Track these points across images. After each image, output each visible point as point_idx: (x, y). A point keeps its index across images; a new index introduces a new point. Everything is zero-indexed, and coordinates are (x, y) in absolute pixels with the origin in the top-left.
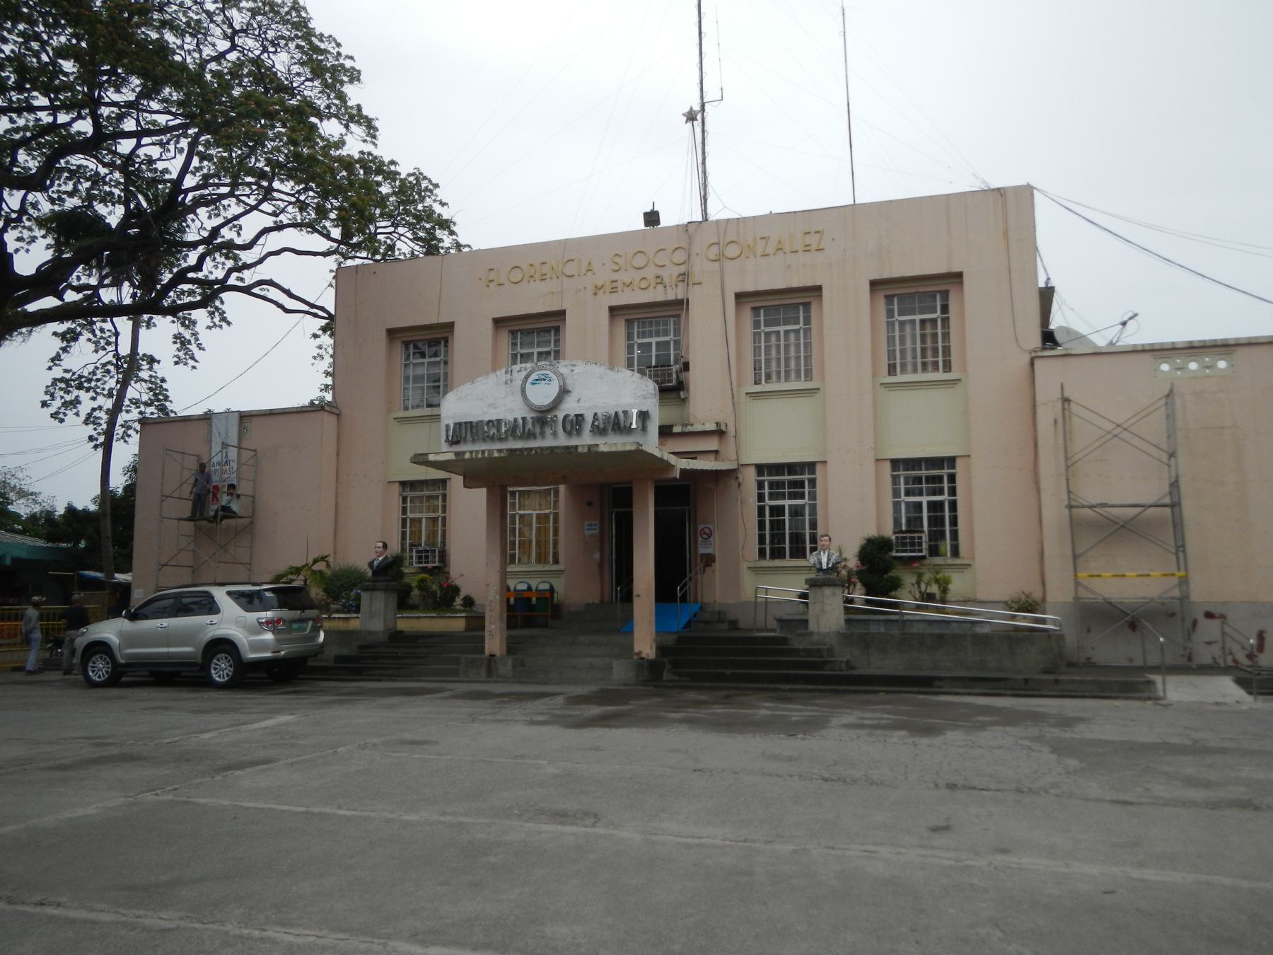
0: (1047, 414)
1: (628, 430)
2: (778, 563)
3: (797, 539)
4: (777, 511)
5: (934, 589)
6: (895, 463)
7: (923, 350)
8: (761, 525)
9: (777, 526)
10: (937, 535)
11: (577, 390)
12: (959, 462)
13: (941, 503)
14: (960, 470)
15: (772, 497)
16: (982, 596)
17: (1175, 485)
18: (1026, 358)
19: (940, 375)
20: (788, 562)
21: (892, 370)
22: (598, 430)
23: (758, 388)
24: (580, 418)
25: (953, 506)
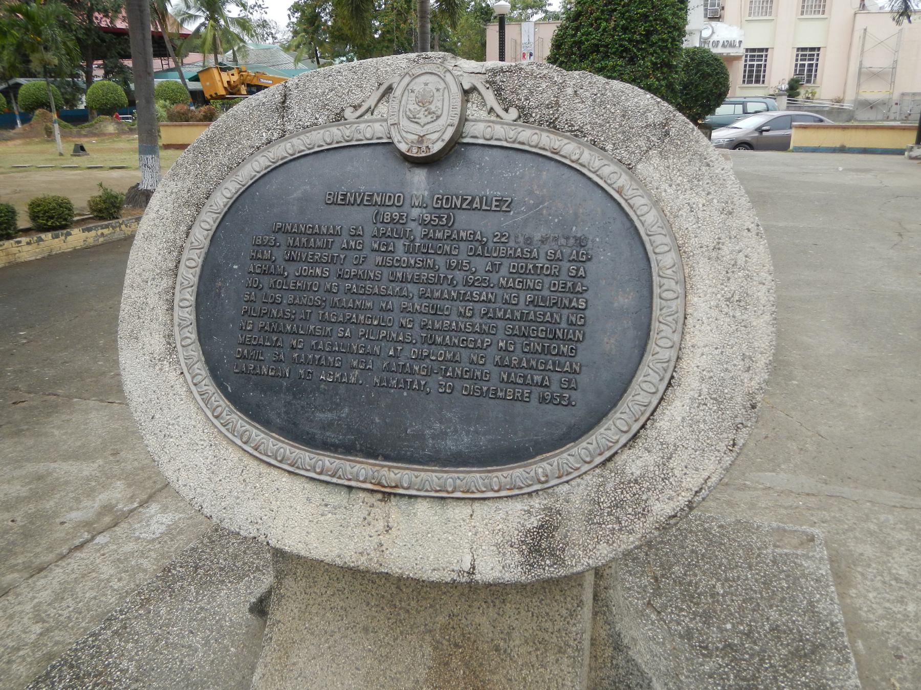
0: (858, 34)
1: (735, 46)
2: (750, 85)
3: (758, 77)
4: (752, 66)
5: (810, 95)
6: (798, 49)
7: (815, 6)
8: (745, 71)
9: (751, 71)
10: (809, 76)
11: (717, 32)
12: (821, 50)
13: (812, 64)
14: (821, 52)
15: (750, 61)
16: (822, 98)
17: (896, 62)
18: (853, 12)
19: (820, 16)
20: (754, 85)
21: (802, 13)
22: (724, 46)
23: (750, 18)
24: (718, 41)
25: (817, 65)
